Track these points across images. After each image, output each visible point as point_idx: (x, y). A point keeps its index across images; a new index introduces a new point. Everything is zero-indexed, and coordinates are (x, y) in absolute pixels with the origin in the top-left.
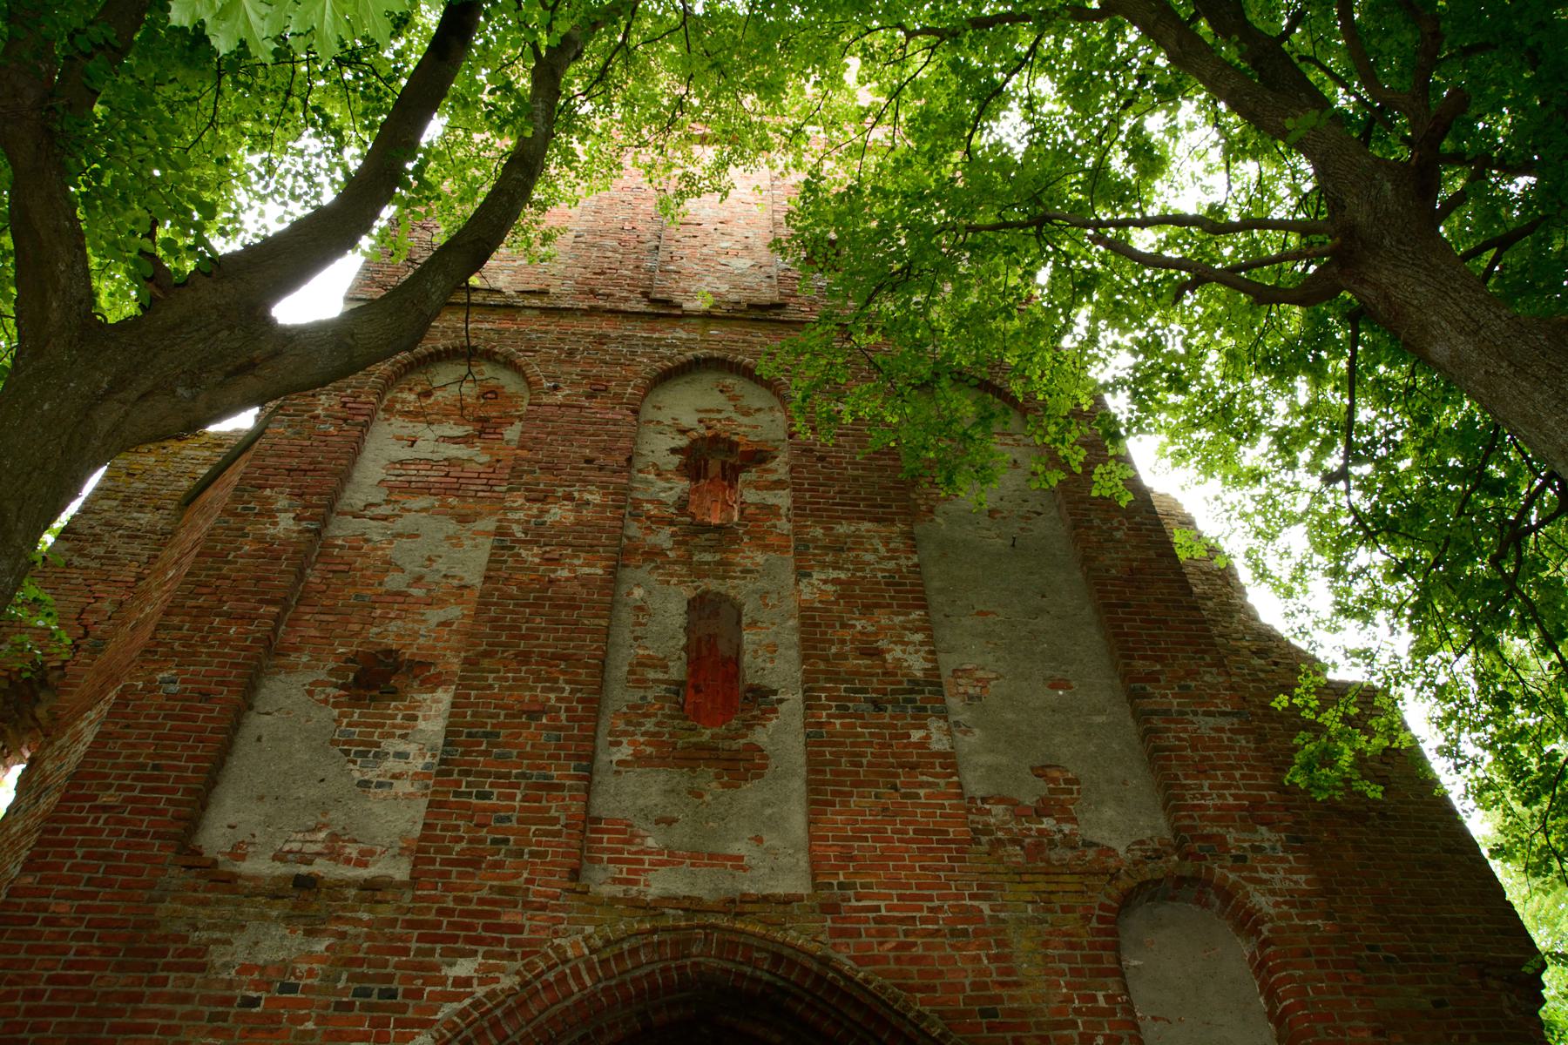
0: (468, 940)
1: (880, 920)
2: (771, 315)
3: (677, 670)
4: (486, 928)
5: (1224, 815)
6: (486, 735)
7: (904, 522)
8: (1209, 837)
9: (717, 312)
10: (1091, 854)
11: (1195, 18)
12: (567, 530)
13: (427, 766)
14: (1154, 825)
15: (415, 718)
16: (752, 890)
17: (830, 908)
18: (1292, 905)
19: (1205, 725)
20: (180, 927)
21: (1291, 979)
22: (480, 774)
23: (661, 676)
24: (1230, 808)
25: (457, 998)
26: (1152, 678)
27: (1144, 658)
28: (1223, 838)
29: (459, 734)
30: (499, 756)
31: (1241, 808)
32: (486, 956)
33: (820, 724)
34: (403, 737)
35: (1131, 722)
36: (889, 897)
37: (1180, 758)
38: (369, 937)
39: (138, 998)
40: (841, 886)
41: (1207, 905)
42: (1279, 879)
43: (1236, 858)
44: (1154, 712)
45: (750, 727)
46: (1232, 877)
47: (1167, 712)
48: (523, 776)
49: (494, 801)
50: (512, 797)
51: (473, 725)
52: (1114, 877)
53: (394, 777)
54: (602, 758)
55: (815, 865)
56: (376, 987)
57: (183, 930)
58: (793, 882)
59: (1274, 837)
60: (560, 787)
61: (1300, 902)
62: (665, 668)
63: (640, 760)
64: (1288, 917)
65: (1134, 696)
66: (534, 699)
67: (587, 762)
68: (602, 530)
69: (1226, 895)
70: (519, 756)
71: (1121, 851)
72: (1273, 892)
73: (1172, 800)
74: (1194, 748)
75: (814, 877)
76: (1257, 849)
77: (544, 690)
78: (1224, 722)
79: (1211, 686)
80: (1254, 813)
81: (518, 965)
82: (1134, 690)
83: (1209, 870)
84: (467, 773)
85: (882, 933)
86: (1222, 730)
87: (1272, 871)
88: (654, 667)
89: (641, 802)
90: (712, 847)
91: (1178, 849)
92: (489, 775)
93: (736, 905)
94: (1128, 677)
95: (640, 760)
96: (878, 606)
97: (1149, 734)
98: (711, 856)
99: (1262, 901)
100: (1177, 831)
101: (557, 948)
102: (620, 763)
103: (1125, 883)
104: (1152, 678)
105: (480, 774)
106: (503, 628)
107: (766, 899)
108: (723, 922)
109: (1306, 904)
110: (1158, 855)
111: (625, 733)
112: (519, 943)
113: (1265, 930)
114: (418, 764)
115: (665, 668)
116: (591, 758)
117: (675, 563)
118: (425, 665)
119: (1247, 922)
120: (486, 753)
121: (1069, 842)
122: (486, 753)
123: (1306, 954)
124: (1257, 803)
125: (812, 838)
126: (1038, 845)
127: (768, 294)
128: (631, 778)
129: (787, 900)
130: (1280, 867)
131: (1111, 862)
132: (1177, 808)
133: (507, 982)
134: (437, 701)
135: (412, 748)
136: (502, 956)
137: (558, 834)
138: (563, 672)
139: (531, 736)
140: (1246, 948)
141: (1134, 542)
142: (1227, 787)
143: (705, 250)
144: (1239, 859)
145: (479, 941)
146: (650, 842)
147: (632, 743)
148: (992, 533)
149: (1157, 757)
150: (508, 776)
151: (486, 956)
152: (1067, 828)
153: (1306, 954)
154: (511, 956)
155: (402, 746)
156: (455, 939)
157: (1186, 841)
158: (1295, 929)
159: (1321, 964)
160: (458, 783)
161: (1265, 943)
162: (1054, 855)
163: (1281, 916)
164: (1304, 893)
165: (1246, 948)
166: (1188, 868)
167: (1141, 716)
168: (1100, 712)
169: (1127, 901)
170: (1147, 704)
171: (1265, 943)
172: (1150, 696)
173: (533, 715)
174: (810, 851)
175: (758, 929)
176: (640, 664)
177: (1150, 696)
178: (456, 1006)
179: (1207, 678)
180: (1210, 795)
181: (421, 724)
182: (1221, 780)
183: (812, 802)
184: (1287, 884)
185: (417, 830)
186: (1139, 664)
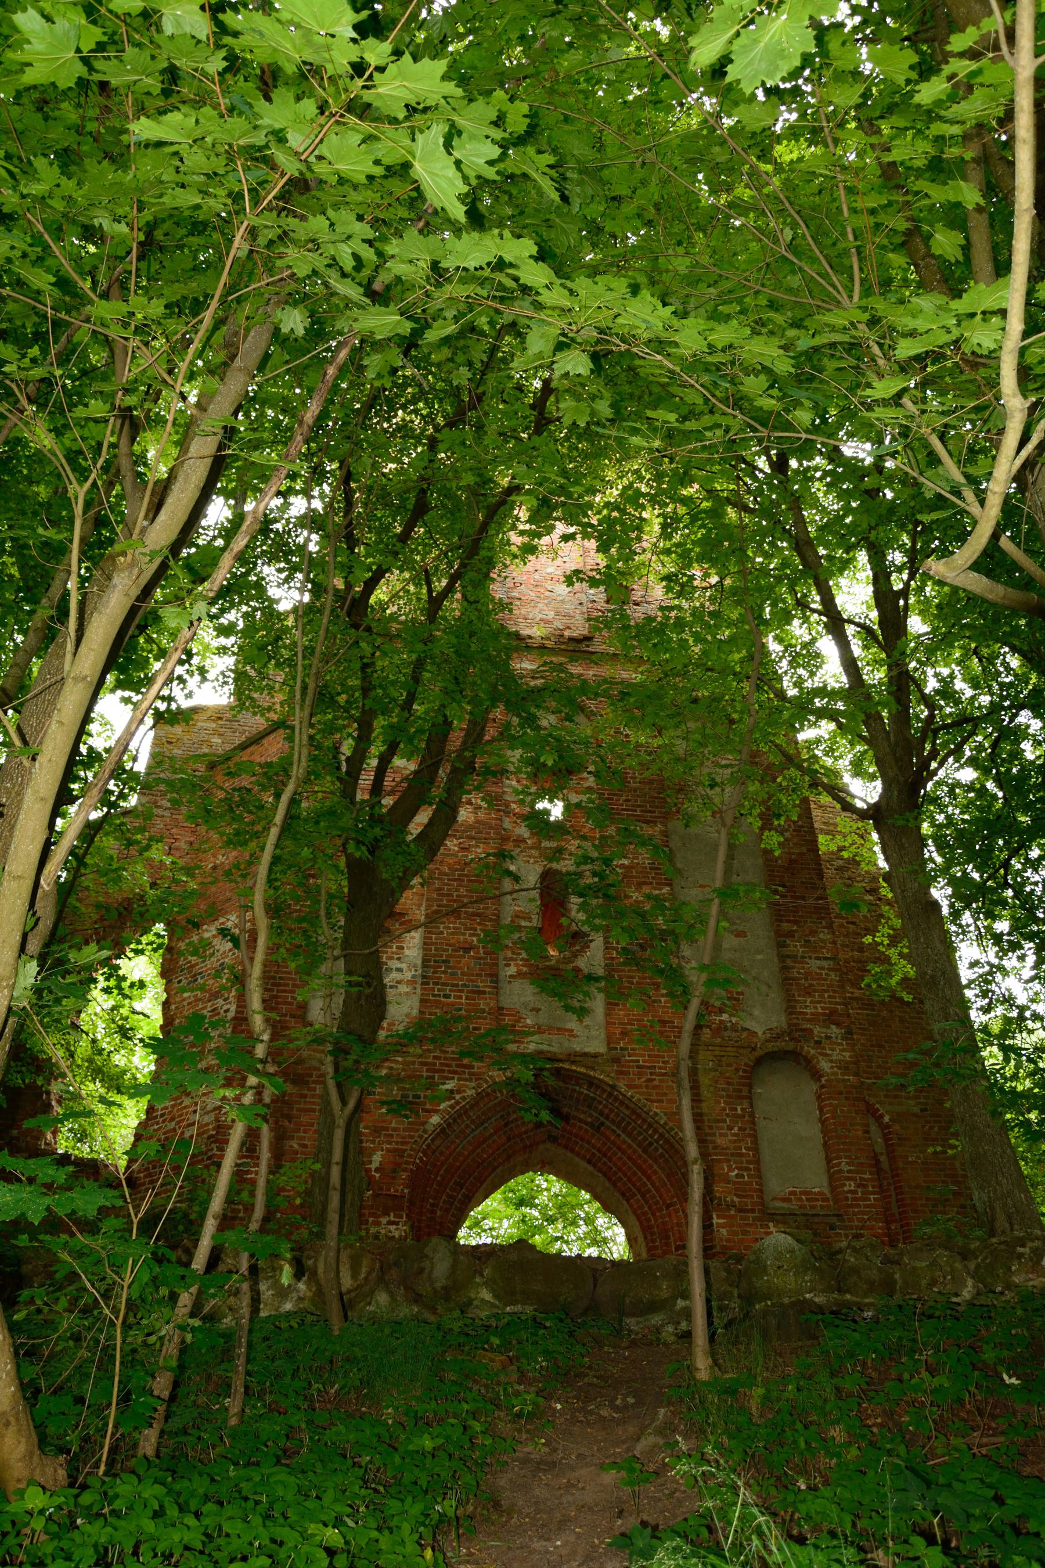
0: (450, 1072)
1: (639, 1067)
2: (583, 647)
3: (536, 921)
4: (457, 1066)
5: (814, 1019)
6: (444, 962)
7: (662, 823)
8: (804, 1030)
9: (549, 644)
10: (745, 1035)
11: (695, 1162)
12: (471, 827)
13: (414, 976)
14: (778, 1020)
15: (402, 948)
16: (577, 1048)
17: (616, 1060)
18: (839, 1068)
19: (814, 964)
20: (316, 1064)
21: (831, 1105)
22: (443, 984)
23: (528, 924)
24: (818, 1014)
25: (449, 1099)
26: (791, 935)
27: (788, 921)
28: (811, 1030)
29: (429, 961)
30: (452, 974)
31: (823, 1014)
32: (459, 1079)
33: (613, 959)
34: (399, 959)
35: (776, 959)
36: (643, 1055)
37: (798, 984)
38: (404, 1070)
39: (305, 1096)
40: (622, 1049)
41: (799, 1063)
42: (836, 1055)
43: (817, 1042)
44: (788, 956)
45: (576, 956)
46: (812, 1052)
47: (795, 956)
48: (464, 985)
49: (452, 999)
50: (460, 997)
51: (435, 955)
52: (754, 1049)
53: (399, 982)
54: (502, 974)
55: (609, 1040)
56: (411, 1094)
57: (317, 1065)
58: (597, 1046)
59: (838, 1031)
60: (484, 992)
61: (844, 1067)
62: (530, 919)
63: (520, 975)
64: (836, 1074)
65: (781, 945)
66: (465, 941)
67: (494, 977)
68: (491, 828)
69: (808, 1061)
70: (463, 974)
71: (760, 1033)
72: (831, 1061)
73: (790, 1008)
74: (806, 979)
75: (608, 1044)
76: (828, 1038)
77: (471, 935)
78: (825, 964)
79: (822, 941)
80: (831, 1018)
81: (473, 1084)
82: (781, 939)
83: (802, 1048)
84: (437, 984)
85: (640, 1074)
86: (822, 968)
87: (833, 1050)
88: (524, 918)
89: (522, 999)
90: (559, 1025)
91: (789, 1034)
92: (447, 985)
93: (574, 1057)
94: (779, 933)
95: (520, 975)
96: (645, 883)
97: (785, 968)
98: (559, 1029)
99: (825, 1065)
100: (789, 1025)
101: (491, 1077)
102: (511, 976)
103: (759, 1053)
104: (791, 935)
105: (443, 984)
106: (443, 895)
107: (586, 1054)
108: (567, 1066)
109: (847, 1068)
110: (778, 1037)
111: (512, 959)
112: (473, 1074)
113: (823, 1080)
114: (408, 975)
115: (530, 919)
116: (496, 976)
117: (532, 848)
118: (403, 915)
119: (816, 1075)
120: (444, 972)
121: (734, 1028)
122: (444, 972)
123: (841, 1093)
124: (833, 1012)
125: (608, 1023)
126: (719, 1029)
127: (580, 629)
128: (517, 985)
129: (596, 1056)
130: (838, 1048)
131: (755, 1040)
132: (791, 1013)
133: (470, 1092)
134: (413, 938)
135: (404, 966)
136: (466, 1080)
137: (485, 1018)
138: (479, 924)
139: (467, 961)
140: (815, 1087)
141: (795, 840)
142: (819, 1002)
143: (537, 576)
144: (819, 1042)
145: (455, 1072)
146: (529, 1021)
147: (516, 965)
148: (712, 829)
149: (787, 982)
150: (457, 985)
151: (459, 1079)
152: (734, 1020)
153: (841, 1093)
154: (470, 1080)
155: (399, 966)
156: (443, 1071)
157: (796, 1031)
158: (838, 1081)
159: (847, 1098)
160: (433, 989)
161: (823, 1087)
162: (726, 1034)
163: (833, 1074)
164: (848, 1062)
165: (815, 1087)
166: (791, 1046)
167: (782, 958)
168: (759, 952)
169: (759, 1061)
170: (785, 951)
171: (823, 1087)
172: (787, 946)
173: (467, 950)
174: (606, 1029)
175: (583, 1070)
176: (517, 916)
177: (787, 946)
178: (448, 1103)
179: (821, 936)
180: (809, 1006)
181: (407, 952)
182: (817, 999)
183: (609, 1003)
184: (840, 1057)
185: (415, 1012)
186: (785, 925)
